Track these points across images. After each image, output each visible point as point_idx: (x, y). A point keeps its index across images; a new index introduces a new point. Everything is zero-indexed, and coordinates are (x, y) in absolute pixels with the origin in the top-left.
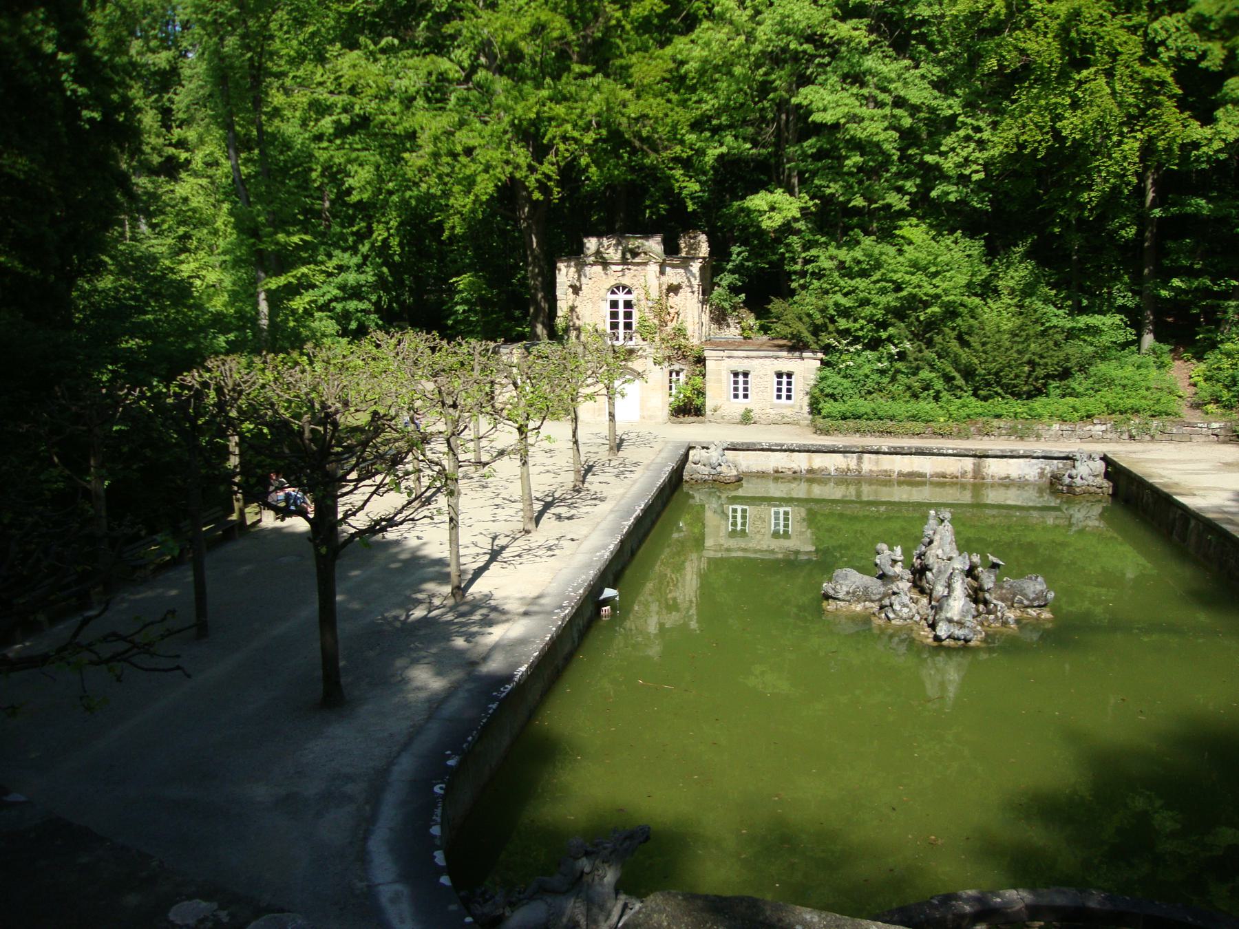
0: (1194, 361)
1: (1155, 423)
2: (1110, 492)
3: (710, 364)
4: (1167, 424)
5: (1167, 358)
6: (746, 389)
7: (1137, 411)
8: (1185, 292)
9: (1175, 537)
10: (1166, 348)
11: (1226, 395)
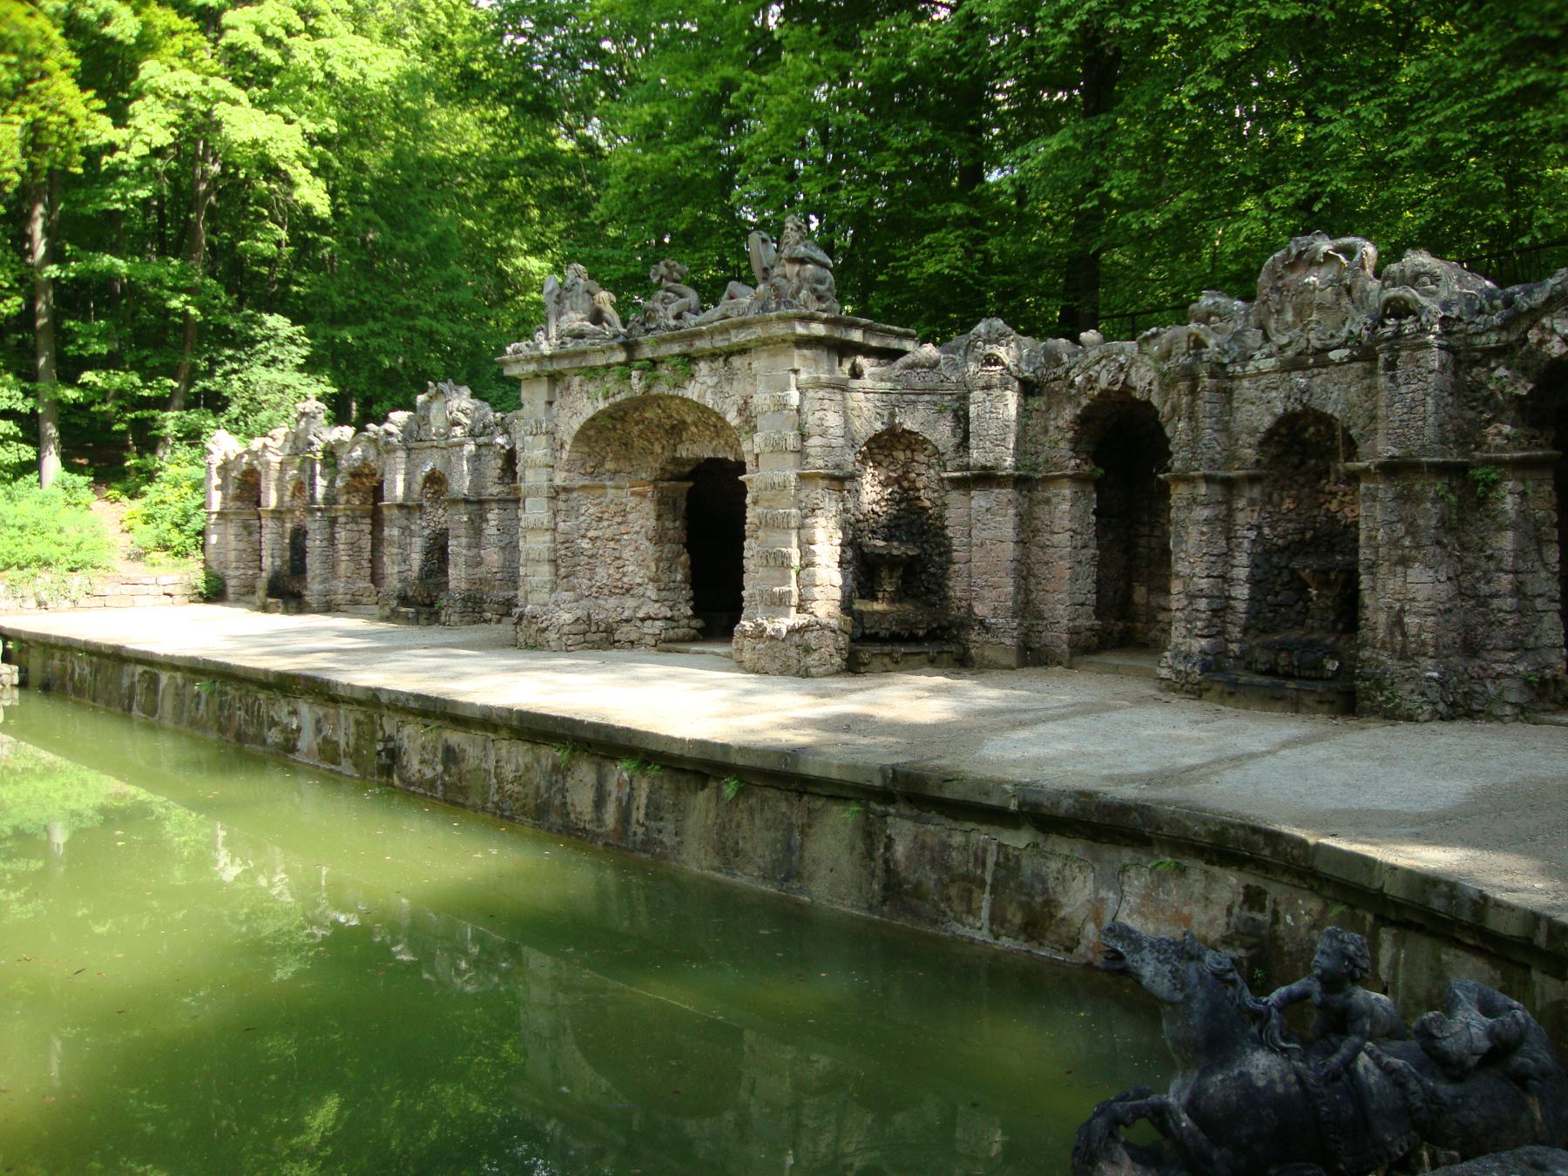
0: (125, 499)
1: (76, 580)
2: (16, 681)
4: (95, 581)
5: (86, 495)
7: (47, 564)
8: (104, 395)
9: (136, 712)
10: (82, 480)
11: (176, 538)
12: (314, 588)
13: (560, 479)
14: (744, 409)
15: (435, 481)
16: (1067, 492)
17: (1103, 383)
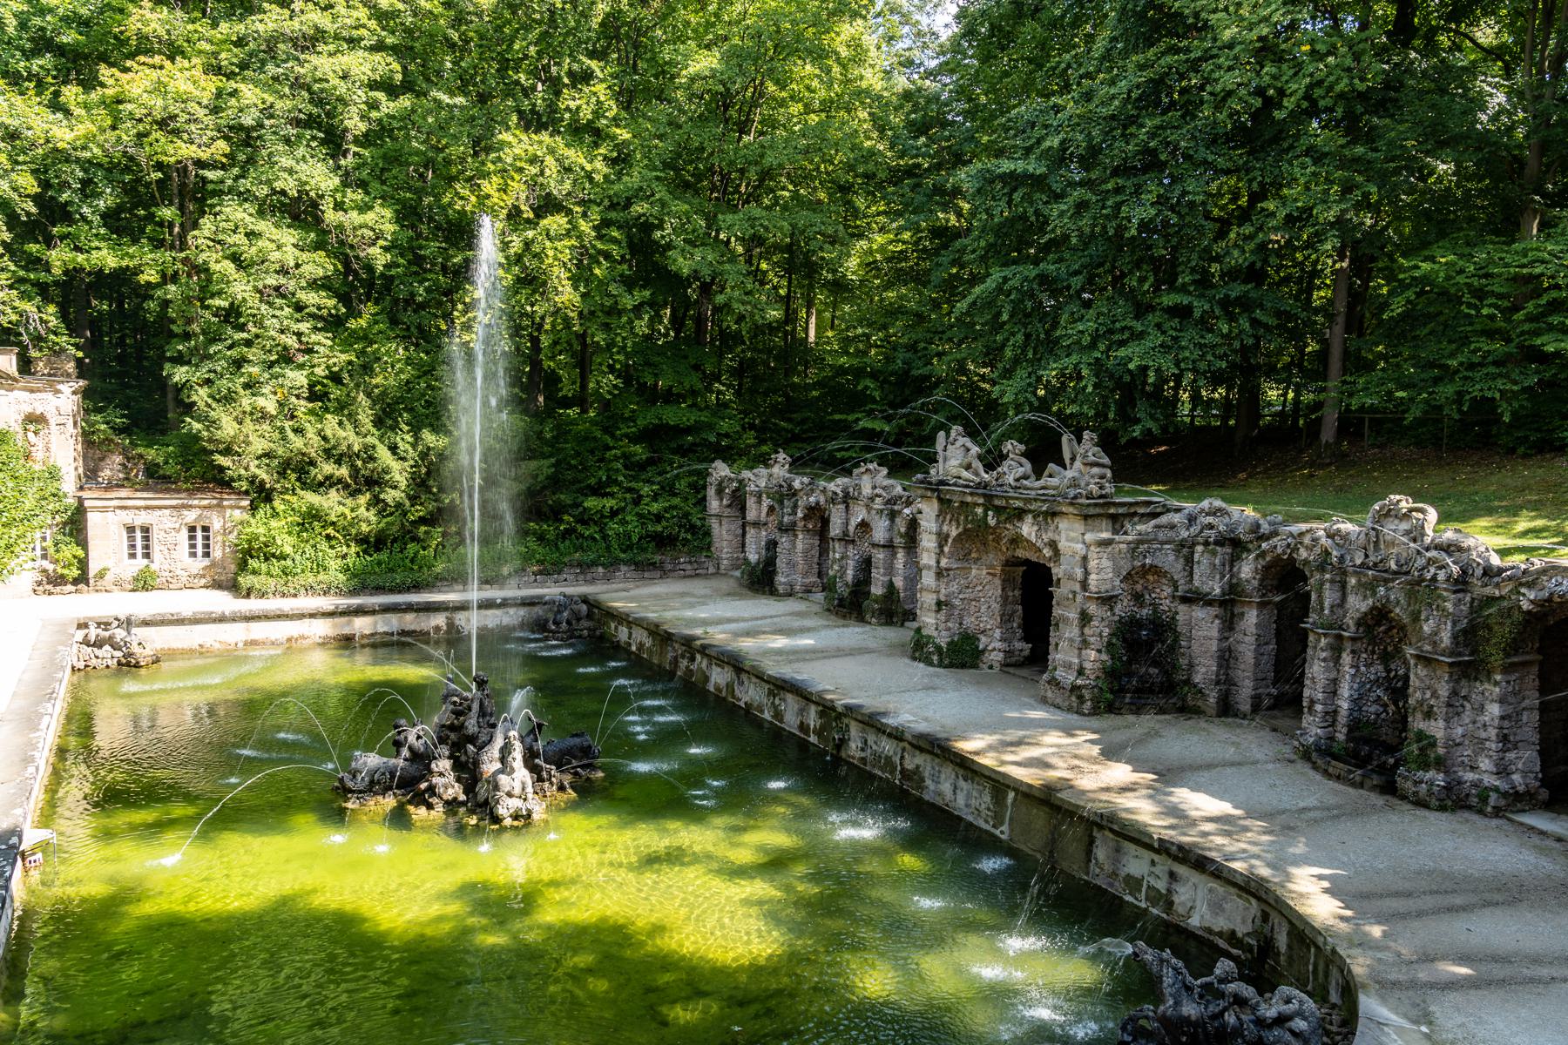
3: (93, 519)
6: (147, 547)
12: (781, 579)
13: (944, 562)
14: (1053, 545)
15: (864, 526)
16: (1255, 612)
17: (1279, 550)
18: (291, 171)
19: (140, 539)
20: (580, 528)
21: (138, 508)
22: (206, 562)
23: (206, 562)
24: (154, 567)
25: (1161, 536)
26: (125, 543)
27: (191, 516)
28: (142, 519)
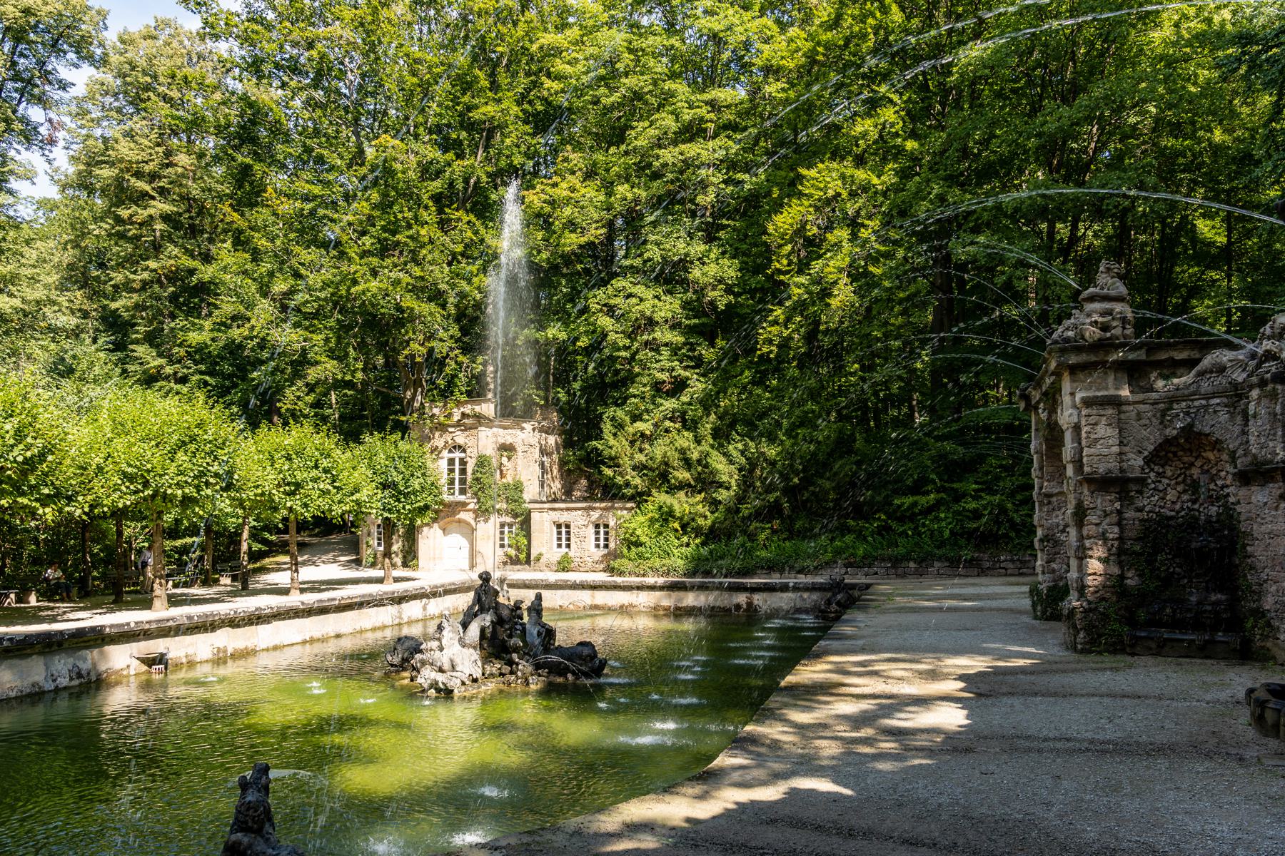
18: (658, 244)
19: (563, 529)
20: (893, 524)
21: (562, 510)
22: (606, 551)
23: (606, 551)
24: (571, 554)
25: (1205, 386)
26: (555, 536)
27: (595, 515)
28: (564, 517)
